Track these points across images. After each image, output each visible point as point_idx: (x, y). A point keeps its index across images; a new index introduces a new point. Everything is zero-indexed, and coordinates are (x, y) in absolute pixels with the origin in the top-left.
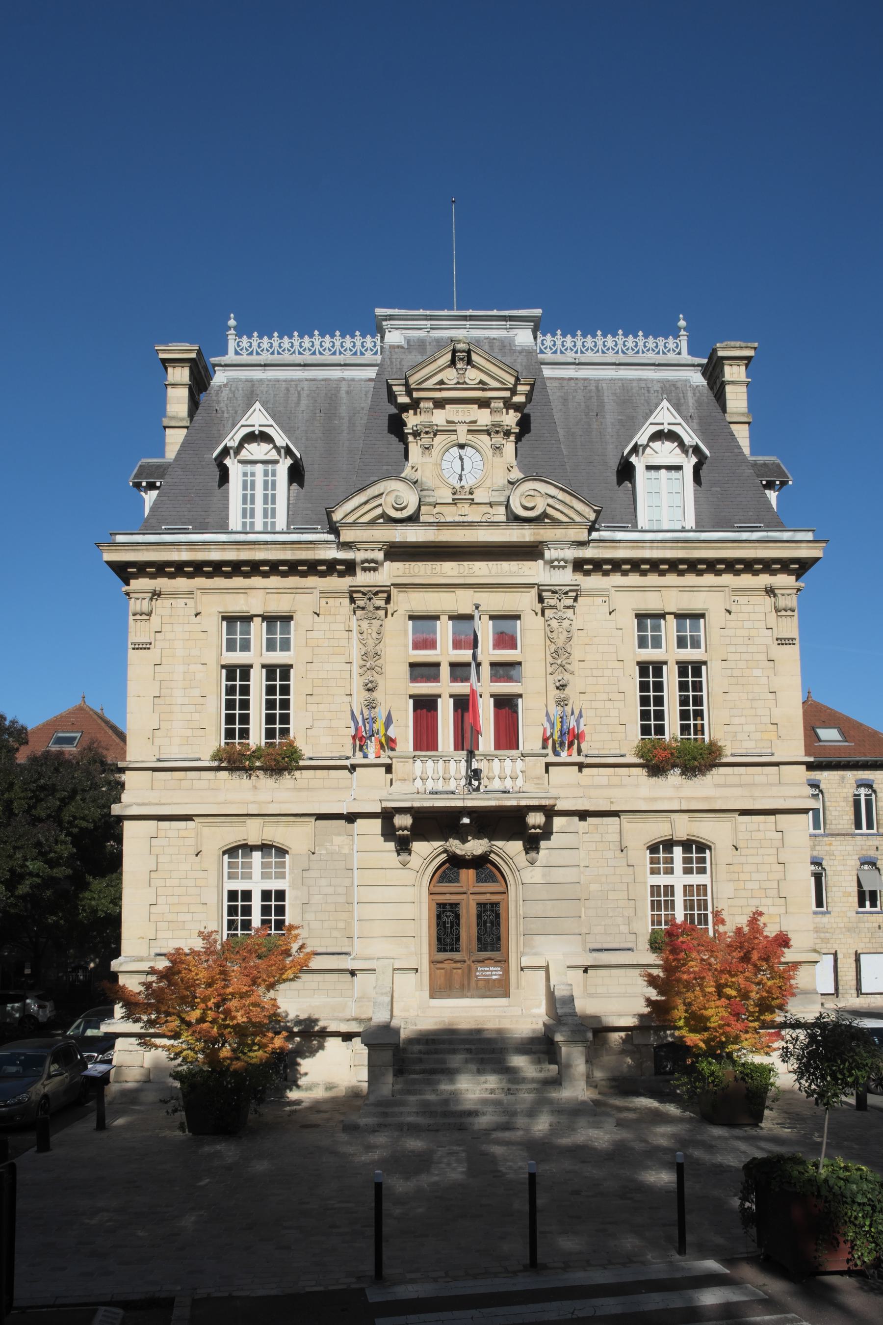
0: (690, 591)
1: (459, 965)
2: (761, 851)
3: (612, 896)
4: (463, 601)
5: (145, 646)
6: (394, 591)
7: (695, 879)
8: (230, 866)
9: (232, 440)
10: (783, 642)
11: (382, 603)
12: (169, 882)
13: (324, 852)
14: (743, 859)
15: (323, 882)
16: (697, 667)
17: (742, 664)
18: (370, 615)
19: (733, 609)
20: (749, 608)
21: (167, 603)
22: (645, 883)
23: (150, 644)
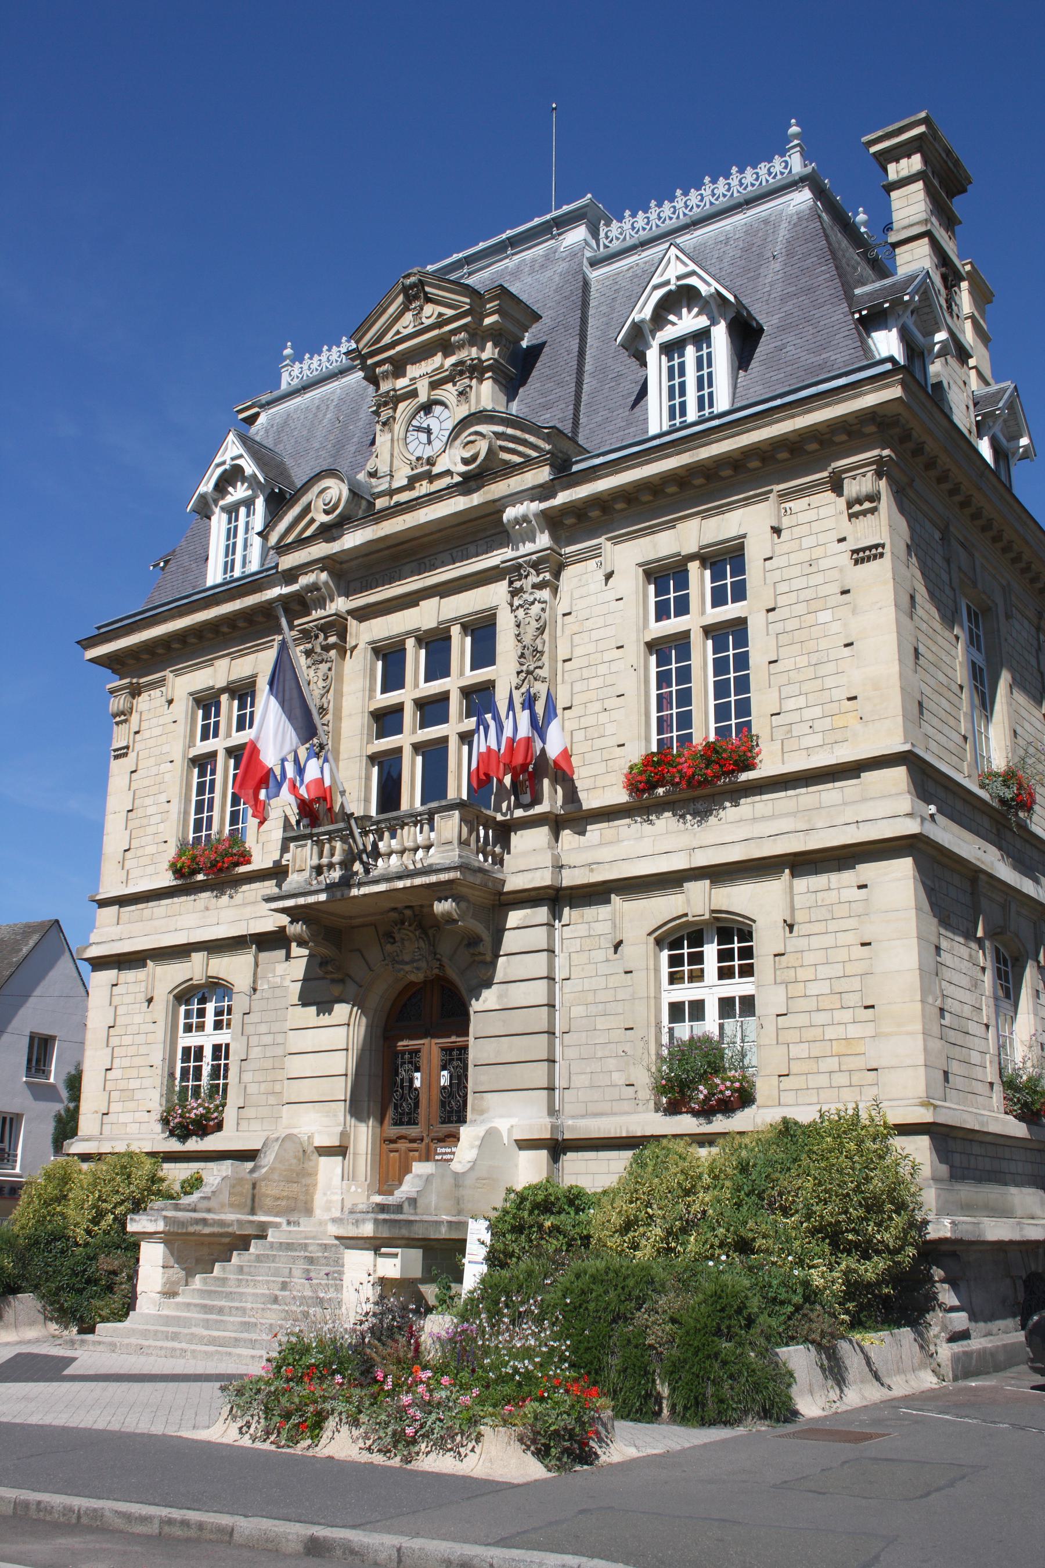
0: (718, 514)
1: (415, 1145)
2: (833, 926)
3: (601, 1023)
4: (426, 615)
5: (122, 753)
6: (352, 623)
7: (738, 988)
8: (188, 1014)
9: (207, 486)
10: (863, 555)
11: (333, 639)
12: (127, 1040)
13: (266, 987)
14: (802, 943)
15: (263, 1028)
16: (738, 628)
17: (801, 608)
18: (316, 657)
19: (786, 522)
20: (811, 515)
21: (144, 696)
22: (658, 999)
23: (127, 747)
